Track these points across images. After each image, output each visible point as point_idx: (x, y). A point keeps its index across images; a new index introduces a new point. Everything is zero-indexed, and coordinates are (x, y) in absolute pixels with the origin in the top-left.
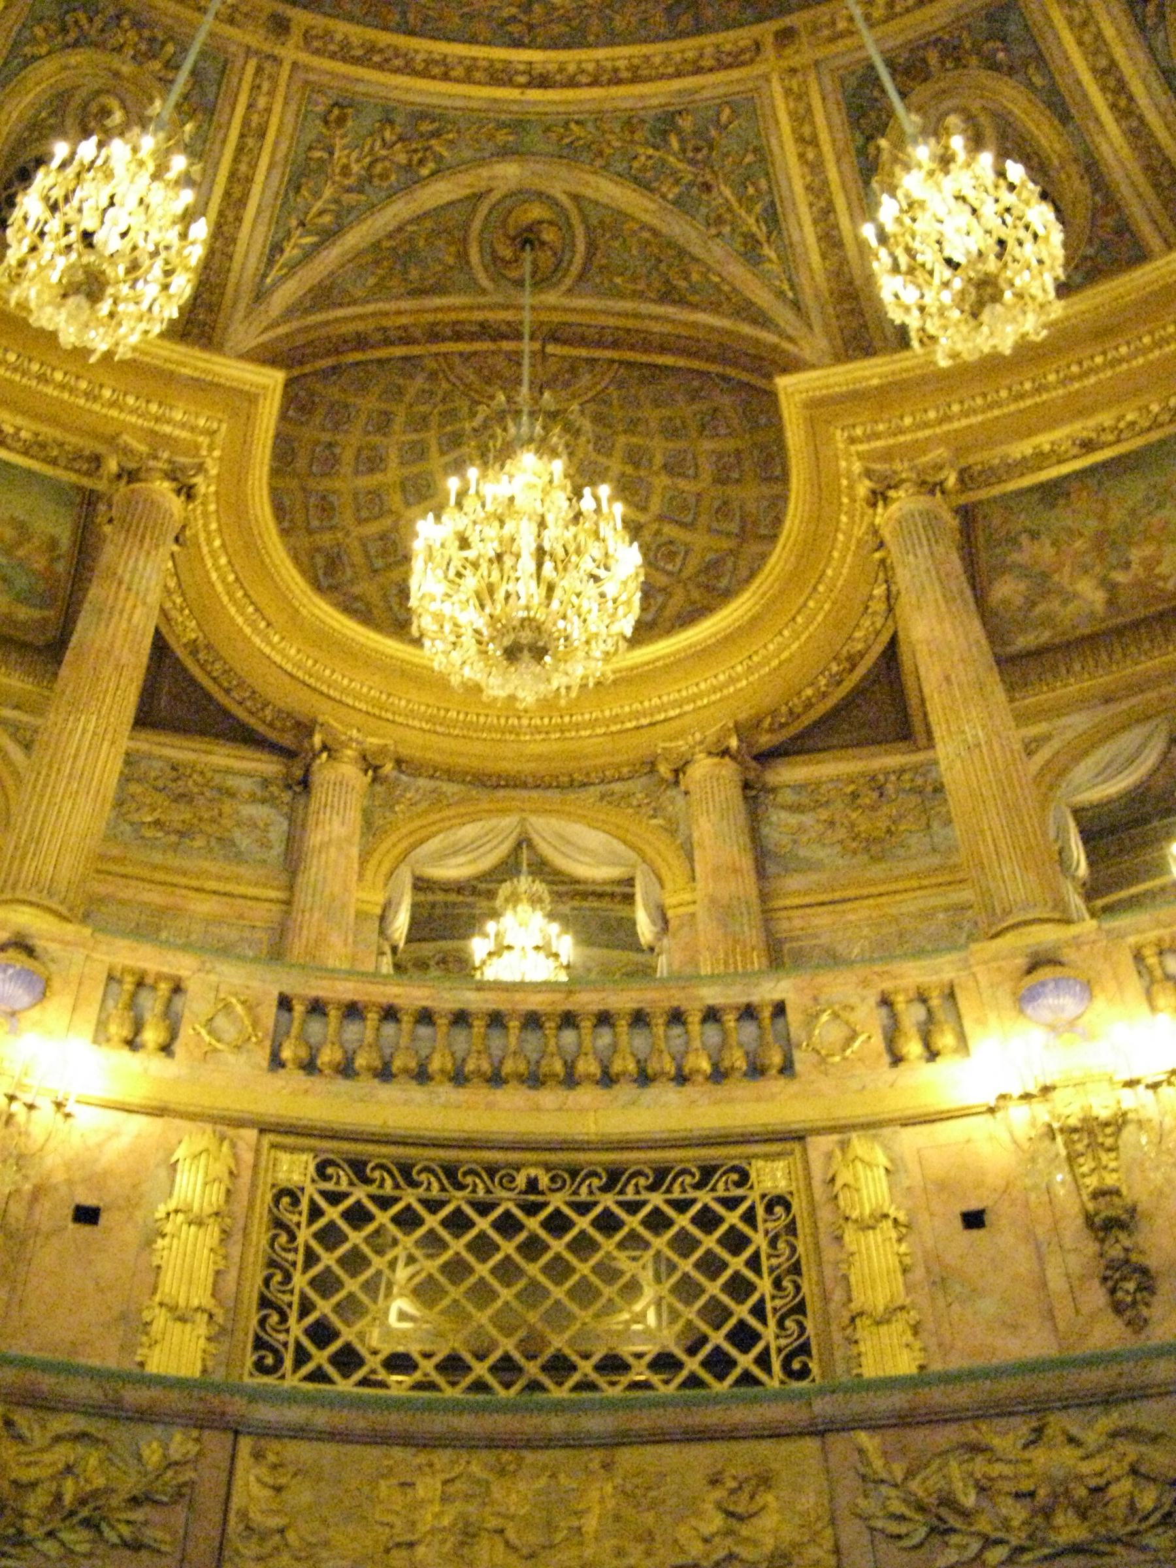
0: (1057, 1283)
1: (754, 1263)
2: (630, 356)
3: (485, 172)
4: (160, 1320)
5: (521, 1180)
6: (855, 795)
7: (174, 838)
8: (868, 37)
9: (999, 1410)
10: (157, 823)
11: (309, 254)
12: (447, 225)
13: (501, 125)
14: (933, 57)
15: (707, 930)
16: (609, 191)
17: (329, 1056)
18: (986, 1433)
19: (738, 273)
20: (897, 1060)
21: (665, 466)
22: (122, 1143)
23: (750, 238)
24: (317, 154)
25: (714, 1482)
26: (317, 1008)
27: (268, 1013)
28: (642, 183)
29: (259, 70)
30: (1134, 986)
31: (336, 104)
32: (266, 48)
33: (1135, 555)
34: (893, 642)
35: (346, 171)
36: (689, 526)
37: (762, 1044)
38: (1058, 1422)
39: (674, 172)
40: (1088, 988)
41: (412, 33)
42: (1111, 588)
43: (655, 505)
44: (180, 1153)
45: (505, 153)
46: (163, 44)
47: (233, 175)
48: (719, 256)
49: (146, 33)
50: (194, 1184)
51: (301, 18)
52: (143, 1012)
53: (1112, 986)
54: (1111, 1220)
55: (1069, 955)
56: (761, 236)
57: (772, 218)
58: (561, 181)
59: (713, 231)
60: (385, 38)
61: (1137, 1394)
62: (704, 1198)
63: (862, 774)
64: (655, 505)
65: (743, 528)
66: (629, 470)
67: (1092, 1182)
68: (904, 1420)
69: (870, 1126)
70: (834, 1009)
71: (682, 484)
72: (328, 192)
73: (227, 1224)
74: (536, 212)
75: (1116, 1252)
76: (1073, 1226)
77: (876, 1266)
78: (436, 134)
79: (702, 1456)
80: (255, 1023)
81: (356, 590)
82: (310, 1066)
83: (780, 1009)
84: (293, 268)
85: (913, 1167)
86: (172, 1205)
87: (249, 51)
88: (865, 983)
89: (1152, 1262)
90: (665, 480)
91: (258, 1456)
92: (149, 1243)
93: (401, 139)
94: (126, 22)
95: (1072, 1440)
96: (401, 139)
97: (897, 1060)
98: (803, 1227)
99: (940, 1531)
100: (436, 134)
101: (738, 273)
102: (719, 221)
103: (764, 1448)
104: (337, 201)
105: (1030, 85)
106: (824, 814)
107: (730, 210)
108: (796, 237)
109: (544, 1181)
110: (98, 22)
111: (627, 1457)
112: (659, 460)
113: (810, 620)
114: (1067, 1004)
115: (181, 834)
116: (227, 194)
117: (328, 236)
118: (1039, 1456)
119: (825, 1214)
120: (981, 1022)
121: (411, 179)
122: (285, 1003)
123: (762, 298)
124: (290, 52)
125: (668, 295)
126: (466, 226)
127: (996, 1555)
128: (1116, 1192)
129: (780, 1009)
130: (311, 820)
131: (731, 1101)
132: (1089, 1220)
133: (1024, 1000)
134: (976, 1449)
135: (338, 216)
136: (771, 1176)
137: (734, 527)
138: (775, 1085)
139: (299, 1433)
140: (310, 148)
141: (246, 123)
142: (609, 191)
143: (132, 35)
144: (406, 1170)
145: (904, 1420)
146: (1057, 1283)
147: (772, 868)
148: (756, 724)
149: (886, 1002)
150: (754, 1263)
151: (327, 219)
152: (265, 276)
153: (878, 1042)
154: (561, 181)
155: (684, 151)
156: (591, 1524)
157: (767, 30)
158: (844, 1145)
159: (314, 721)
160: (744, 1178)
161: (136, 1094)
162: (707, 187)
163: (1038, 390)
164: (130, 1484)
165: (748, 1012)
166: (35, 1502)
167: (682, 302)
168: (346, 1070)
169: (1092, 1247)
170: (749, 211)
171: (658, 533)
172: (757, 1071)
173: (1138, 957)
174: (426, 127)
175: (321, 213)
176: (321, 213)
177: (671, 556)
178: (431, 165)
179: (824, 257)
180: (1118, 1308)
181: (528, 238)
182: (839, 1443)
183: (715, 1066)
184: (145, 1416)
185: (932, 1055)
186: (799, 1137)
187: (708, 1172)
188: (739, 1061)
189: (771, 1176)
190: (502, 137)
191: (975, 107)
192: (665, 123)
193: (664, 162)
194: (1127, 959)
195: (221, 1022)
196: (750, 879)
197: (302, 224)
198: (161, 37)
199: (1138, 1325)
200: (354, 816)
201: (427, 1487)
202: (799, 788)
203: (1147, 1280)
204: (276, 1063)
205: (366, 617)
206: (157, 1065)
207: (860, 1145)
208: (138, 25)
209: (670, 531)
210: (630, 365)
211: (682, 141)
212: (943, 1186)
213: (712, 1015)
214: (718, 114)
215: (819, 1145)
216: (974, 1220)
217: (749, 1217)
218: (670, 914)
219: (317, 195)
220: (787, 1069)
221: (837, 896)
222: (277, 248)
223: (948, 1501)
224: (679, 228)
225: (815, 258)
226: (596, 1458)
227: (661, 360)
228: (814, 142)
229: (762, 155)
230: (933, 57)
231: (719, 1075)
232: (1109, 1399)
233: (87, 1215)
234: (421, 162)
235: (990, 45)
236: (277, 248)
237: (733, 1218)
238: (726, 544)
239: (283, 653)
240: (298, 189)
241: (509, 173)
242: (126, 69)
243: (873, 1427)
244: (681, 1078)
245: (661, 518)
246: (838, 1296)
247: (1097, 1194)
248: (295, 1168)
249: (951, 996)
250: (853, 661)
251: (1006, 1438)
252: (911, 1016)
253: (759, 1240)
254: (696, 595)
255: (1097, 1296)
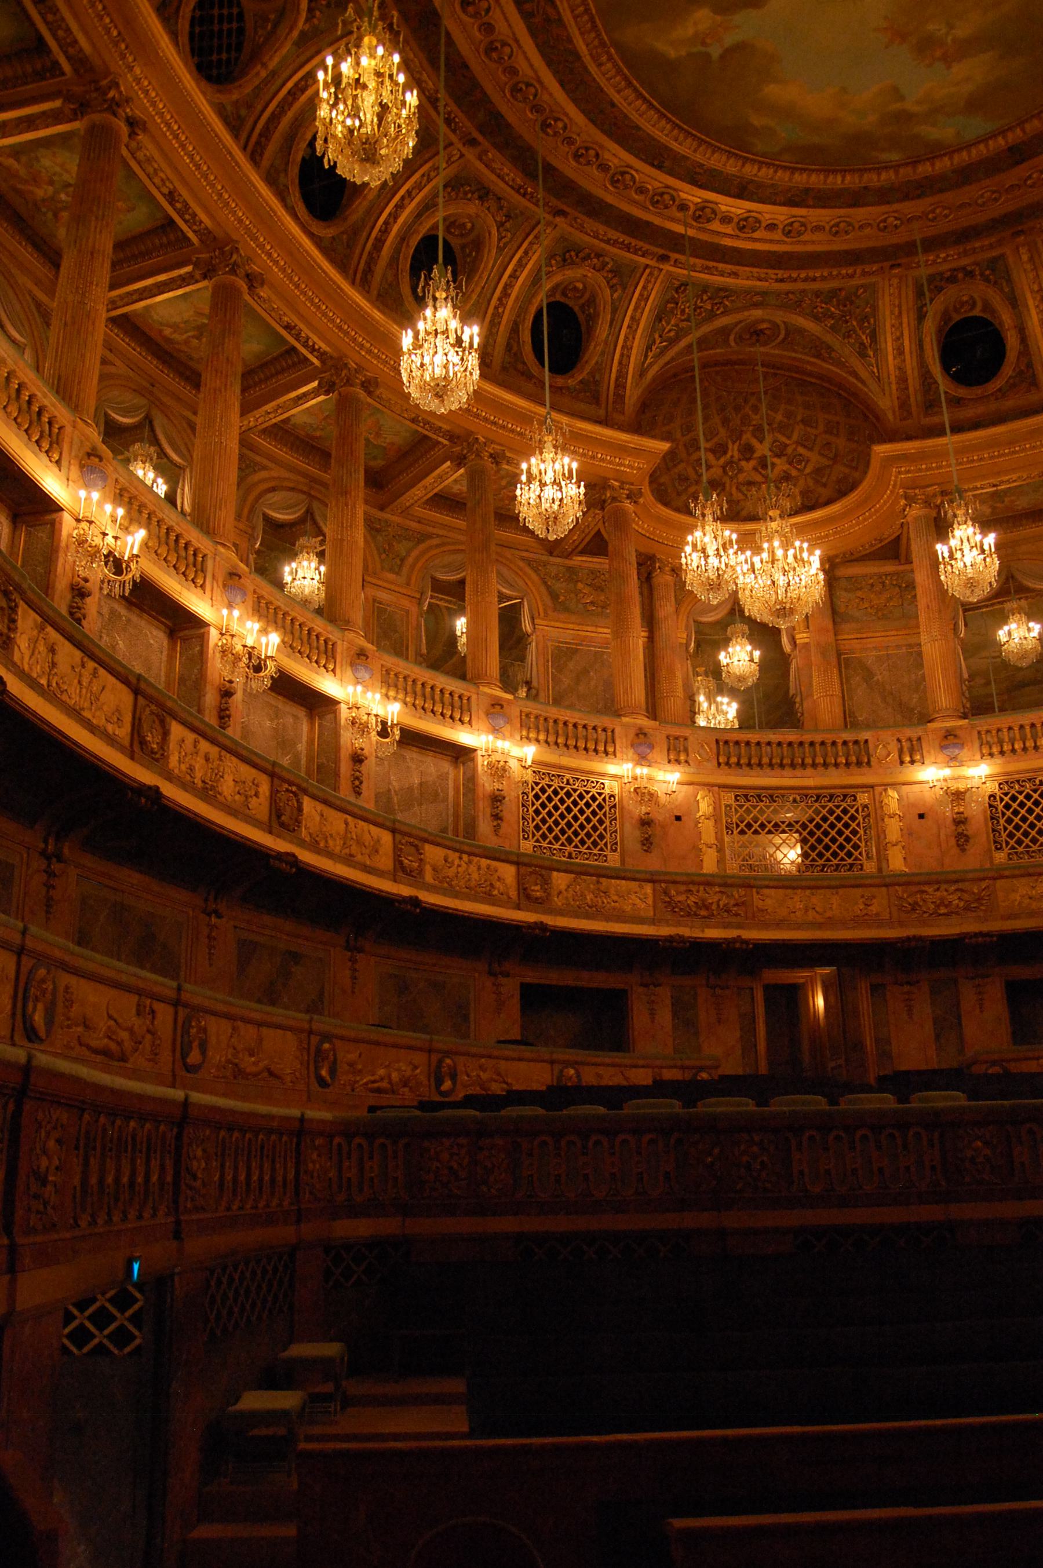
0: (943, 837)
1: (858, 825)
2: (794, 375)
3: (746, 313)
4: (704, 848)
5: (791, 799)
6: (872, 585)
7: (600, 609)
8: (946, 418)
9: (929, 883)
10: (592, 603)
11: (663, 352)
12: (725, 331)
13: (757, 294)
14: (960, 275)
15: (815, 658)
16: (801, 322)
17: (733, 760)
18: (926, 888)
19: (855, 363)
20: (902, 763)
21: (802, 421)
22: (683, 794)
23: (862, 344)
24: (670, 305)
25: (862, 897)
26: (726, 742)
27: (714, 746)
28: (817, 318)
29: (651, 274)
30: (977, 744)
31: (682, 285)
32: (657, 265)
33: (1006, 499)
34: (898, 538)
35: (683, 312)
36: (811, 449)
37: (860, 757)
38: (944, 886)
39: (833, 313)
40: (962, 746)
41: (726, 262)
42: (994, 508)
43: (795, 437)
44: (699, 798)
45: (756, 305)
46: (608, 263)
47: (632, 318)
48: (845, 350)
49: (601, 259)
50: (705, 806)
51: (674, 256)
52: (677, 751)
53: (970, 744)
54: (960, 821)
55: (958, 732)
56: (868, 345)
57: (873, 336)
58: (779, 317)
59: (846, 341)
60: (711, 264)
61: (963, 881)
62: (844, 805)
63: (875, 574)
64: (795, 437)
65: (836, 456)
66: (785, 420)
67: (956, 810)
68: (908, 884)
69: (893, 785)
70: (883, 744)
71: (809, 429)
72: (673, 322)
73: (716, 817)
74: (764, 326)
75: (960, 830)
76: (949, 821)
77: (893, 829)
78: (727, 297)
79: (860, 891)
80: (711, 749)
81: (662, 480)
82: (727, 764)
83: (866, 741)
84: (657, 357)
85: (905, 797)
86: (701, 813)
87: (647, 266)
88: (893, 735)
89: (969, 833)
90: (802, 426)
91: (758, 893)
92: (696, 825)
93: (710, 298)
94: (592, 255)
95: (946, 890)
96: (710, 298)
97: (902, 763)
98: (873, 815)
99: (914, 909)
100: (727, 297)
101: (855, 363)
102: (849, 336)
103: (873, 889)
104: (677, 325)
105: (1002, 290)
106: (859, 594)
107: (855, 332)
108: (883, 346)
109: (798, 798)
110: (581, 255)
111: (841, 891)
112: (799, 418)
113: (865, 520)
114: (957, 751)
115: (603, 607)
116: (629, 327)
117: (673, 342)
118: (938, 894)
119: (879, 811)
120: (929, 752)
121: (712, 316)
122: (717, 741)
123: (864, 374)
124: (667, 267)
125: (818, 356)
126: (731, 330)
127: (925, 915)
128: (962, 813)
129: (866, 741)
130: (657, 604)
131: (852, 775)
132: (954, 820)
133: (943, 748)
134: (923, 892)
135: (677, 333)
136: (863, 798)
137: (831, 455)
138: (865, 770)
139: (768, 887)
140: (668, 302)
141: (641, 295)
142: (801, 322)
143: (595, 261)
144: (759, 796)
145: (908, 884)
146: (943, 837)
147: (838, 620)
148: (836, 556)
149: (899, 740)
150: (858, 825)
151: (672, 334)
152: (644, 363)
153: (897, 756)
154: (779, 317)
155: (838, 305)
156: (834, 907)
157: (887, 265)
158: (885, 790)
159: (654, 555)
160: (855, 800)
161: (686, 778)
162: (847, 322)
163: (981, 460)
164: (732, 902)
165: (856, 742)
166: (714, 907)
167: (823, 360)
168: (738, 764)
169: (954, 828)
170: (864, 333)
171: (795, 449)
172: (859, 764)
173: (979, 732)
174: (722, 294)
175: (670, 331)
176: (670, 331)
177: (800, 462)
178: (722, 309)
179: (895, 358)
180: (958, 845)
181: (759, 333)
182: (891, 889)
183: (847, 760)
184: (731, 886)
185: (912, 762)
186: (872, 787)
187: (845, 796)
188: (854, 759)
189: (863, 798)
190: (756, 299)
191: (976, 296)
192: (834, 293)
193: (829, 310)
194: (975, 733)
195: (701, 751)
196: (832, 634)
197: (660, 336)
198: (607, 259)
199: (963, 850)
200: (673, 599)
201: (797, 898)
202: (849, 579)
203: (967, 839)
204: (719, 764)
205: (677, 510)
206: (687, 769)
207: (890, 792)
208: (598, 256)
209: (801, 450)
210: (792, 377)
211: (838, 301)
212: (913, 805)
213: (845, 743)
214: (857, 290)
215: (878, 789)
216: (921, 816)
217: (857, 811)
218: (798, 642)
219: (668, 323)
220: (869, 763)
221: (864, 636)
222: (649, 348)
223: (916, 903)
224: (829, 338)
225: (890, 358)
226: (834, 891)
227: (809, 379)
228: (900, 306)
229: (875, 308)
230: (960, 275)
231: (848, 764)
232: (956, 881)
233: (678, 818)
234: (718, 309)
235: (987, 272)
236: (649, 348)
237: (852, 811)
238: (825, 462)
239: (643, 529)
240: (660, 320)
241: (757, 313)
242: (589, 275)
243: (899, 885)
244: (836, 765)
245: (797, 443)
246: (882, 837)
247: (958, 813)
248: (728, 798)
249: (919, 739)
250: (881, 541)
251: (930, 890)
252: (906, 745)
253: (860, 818)
254: (811, 482)
255: (953, 841)
